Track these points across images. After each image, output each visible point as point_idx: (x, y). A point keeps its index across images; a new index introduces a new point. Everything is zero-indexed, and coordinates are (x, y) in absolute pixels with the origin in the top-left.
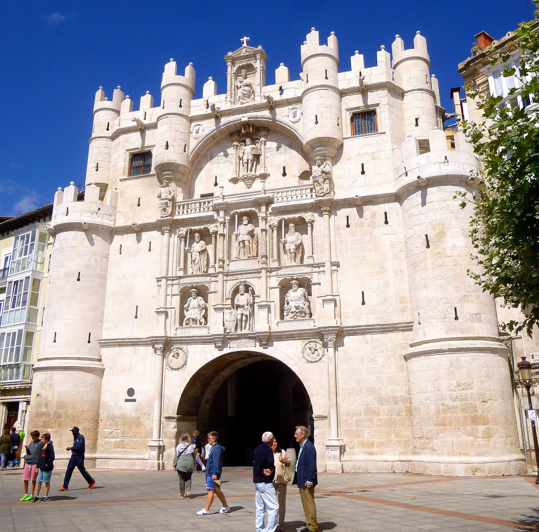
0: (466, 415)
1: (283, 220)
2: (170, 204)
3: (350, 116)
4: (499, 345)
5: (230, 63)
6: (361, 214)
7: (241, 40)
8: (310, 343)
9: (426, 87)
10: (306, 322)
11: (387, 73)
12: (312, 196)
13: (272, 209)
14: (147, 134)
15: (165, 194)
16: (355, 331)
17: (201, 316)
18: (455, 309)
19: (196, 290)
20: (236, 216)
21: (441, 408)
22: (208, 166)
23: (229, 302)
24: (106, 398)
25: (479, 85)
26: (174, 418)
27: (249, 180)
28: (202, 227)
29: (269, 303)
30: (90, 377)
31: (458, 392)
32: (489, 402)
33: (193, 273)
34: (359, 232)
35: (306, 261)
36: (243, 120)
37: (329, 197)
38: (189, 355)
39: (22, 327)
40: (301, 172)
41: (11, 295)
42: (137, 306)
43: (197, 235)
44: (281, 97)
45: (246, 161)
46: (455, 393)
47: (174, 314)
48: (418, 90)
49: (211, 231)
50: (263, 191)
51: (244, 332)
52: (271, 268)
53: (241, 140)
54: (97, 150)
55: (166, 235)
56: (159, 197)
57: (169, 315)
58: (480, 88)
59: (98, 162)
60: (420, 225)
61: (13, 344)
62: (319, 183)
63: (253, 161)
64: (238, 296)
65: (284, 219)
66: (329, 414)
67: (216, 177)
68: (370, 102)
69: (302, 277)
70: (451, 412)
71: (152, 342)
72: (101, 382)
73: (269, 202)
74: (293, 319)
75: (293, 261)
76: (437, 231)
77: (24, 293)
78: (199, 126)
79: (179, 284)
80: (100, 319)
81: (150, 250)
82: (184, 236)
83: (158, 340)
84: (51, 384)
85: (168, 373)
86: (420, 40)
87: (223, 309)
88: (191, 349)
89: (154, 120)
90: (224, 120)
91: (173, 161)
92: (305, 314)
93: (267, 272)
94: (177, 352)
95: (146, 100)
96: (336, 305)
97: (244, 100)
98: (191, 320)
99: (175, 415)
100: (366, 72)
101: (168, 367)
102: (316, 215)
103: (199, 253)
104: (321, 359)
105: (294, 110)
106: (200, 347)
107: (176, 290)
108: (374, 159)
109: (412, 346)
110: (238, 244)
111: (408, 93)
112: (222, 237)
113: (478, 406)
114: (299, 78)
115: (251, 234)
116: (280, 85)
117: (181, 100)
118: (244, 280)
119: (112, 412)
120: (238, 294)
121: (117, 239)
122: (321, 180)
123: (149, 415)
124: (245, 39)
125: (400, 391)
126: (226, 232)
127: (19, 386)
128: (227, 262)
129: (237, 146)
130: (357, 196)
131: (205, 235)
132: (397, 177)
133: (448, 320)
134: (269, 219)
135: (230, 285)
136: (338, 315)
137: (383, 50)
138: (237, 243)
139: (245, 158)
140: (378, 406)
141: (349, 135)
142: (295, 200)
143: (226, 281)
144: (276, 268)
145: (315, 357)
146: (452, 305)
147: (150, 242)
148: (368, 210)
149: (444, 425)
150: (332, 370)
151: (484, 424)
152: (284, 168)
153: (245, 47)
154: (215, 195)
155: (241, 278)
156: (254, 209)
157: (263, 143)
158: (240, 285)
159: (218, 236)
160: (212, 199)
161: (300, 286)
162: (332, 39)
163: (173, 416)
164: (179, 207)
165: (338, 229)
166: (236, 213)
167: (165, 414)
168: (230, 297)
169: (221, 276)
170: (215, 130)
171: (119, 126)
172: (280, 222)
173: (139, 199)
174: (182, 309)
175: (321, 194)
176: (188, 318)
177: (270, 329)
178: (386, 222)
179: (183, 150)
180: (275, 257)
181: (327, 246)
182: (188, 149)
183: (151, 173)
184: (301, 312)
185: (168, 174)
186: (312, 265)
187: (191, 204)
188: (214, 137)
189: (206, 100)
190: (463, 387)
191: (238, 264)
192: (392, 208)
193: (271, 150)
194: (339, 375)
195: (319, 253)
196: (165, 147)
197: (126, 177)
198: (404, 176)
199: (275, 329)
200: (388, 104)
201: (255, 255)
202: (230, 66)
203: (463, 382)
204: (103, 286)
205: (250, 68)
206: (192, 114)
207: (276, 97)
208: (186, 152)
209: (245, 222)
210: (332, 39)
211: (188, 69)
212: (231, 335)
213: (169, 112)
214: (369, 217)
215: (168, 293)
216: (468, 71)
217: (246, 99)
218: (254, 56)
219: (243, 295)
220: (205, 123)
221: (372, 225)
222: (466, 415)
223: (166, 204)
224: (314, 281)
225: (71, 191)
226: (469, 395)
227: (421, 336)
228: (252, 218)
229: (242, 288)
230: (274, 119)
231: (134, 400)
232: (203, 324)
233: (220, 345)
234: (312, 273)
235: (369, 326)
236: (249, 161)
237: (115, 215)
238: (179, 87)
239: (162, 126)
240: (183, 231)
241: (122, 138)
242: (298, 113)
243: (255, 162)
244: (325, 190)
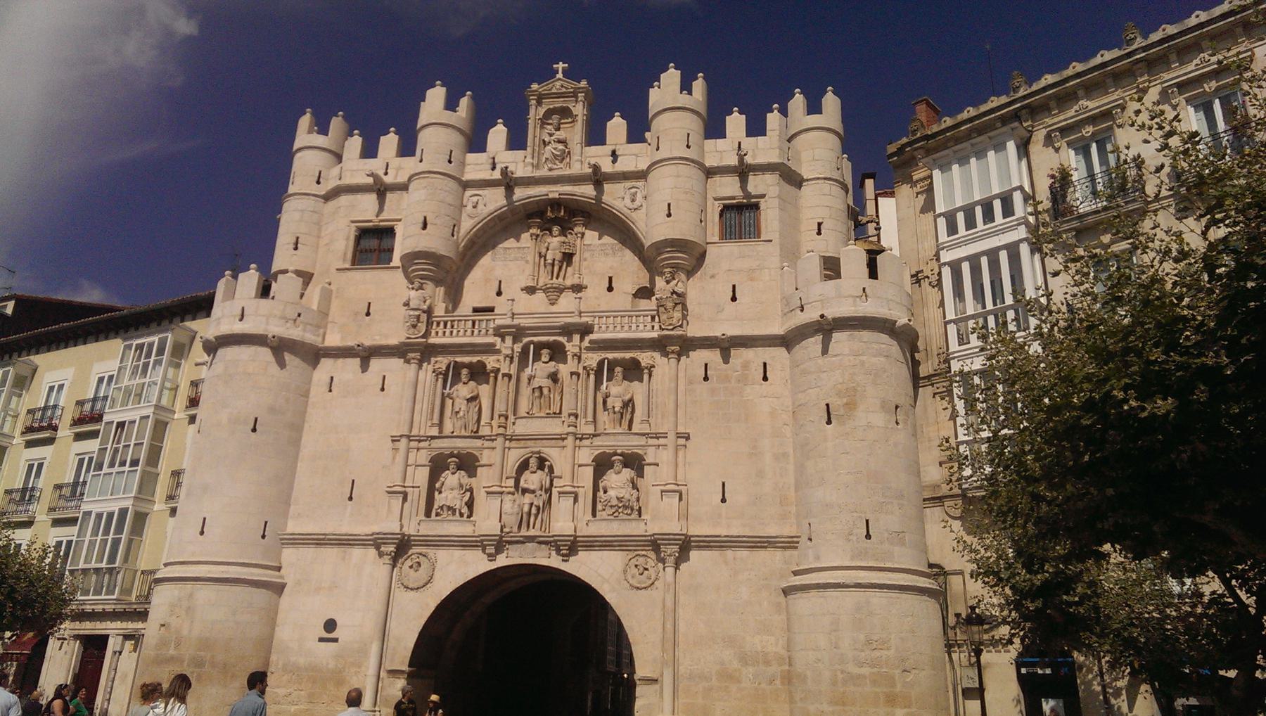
0: (877, 690)
2: (424, 317)
3: (720, 208)
4: (930, 583)
5: (535, 102)
6: (726, 359)
7: (555, 66)
8: (637, 558)
9: (836, 175)
10: (634, 524)
11: (780, 149)
13: (591, 342)
14: (387, 200)
15: (418, 302)
16: (708, 543)
17: (463, 504)
18: (867, 521)
19: (457, 460)
20: (532, 346)
21: (840, 676)
22: (486, 261)
23: (511, 482)
24: (284, 633)
25: (917, 181)
26: (402, 672)
27: (555, 293)
29: (576, 489)
30: (261, 596)
31: (868, 652)
32: (914, 671)
33: (453, 432)
35: (636, 428)
36: (551, 196)
37: (681, 332)
38: (438, 566)
39: (128, 504)
40: (638, 287)
41: (109, 446)
42: (353, 481)
43: (465, 372)
44: (614, 168)
45: (550, 261)
46: (863, 654)
47: (418, 497)
48: (825, 179)
49: (489, 367)
50: (577, 313)
51: (532, 532)
52: (583, 435)
53: (544, 228)
54: (297, 216)
55: (414, 367)
56: (407, 304)
57: (409, 498)
58: (918, 186)
59: (298, 235)
60: (818, 389)
61: (106, 532)
62: (665, 309)
63: (561, 262)
64: (526, 475)
65: (607, 358)
66: (662, 675)
67: (500, 282)
68: (750, 188)
70: (854, 685)
71: (377, 542)
72: (277, 605)
73: (586, 330)
74: (612, 517)
75: (618, 425)
76: (845, 400)
77: (135, 444)
78: (479, 197)
79: (430, 448)
80: (285, 500)
81: (383, 389)
84: (189, 608)
85: (400, 596)
86: (831, 102)
87: (502, 493)
88: (442, 555)
89: (402, 179)
90: (520, 193)
91: (433, 250)
92: (632, 510)
94: (417, 560)
95: (389, 142)
96: (680, 499)
97: (555, 164)
98: (445, 508)
99: (405, 668)
100: (749, 142)
101: (400, 585)
102: (657, 355)
104: (653, 583)
105: (633, 190)
106: (457, 553)
107: (424, 457)
108: (752, 279)
109: (796, 573)
111: (810, 183)
112: (506, 379)
113: (897, 678)
114: (643, 140)
115: (554, 377)
116: (613, 147)
117: (451, 152)
118: (538, 449)
119: (293, 659)
120: (526, 472)
121: (326, 365)
122: (670, 305)
123: (360, 667)
124: (561, 66)
125: (773, 644)
126: (513, 371)
127: (113, 607)
128: (511, 419)
129: (538, 236)
130: (724, 335)
131: (479, 373)
132: (786, 311)
133: (854, 538)
134: (584, 356)
135: (515, 456)
136: (684, 516)
137: (776, 111)
138: (530, 389)
139: (549, 257)
140: (740, 667)
141: (716, 239)
142: (626, 331)
143: (509, 449)
144: (590, 435)
145: (643, 580)
146: (863, 516)
147: (384, 377)
148: (738, 356)
149: (844, 704)
150: (669, 604)
151: (905, 707)
152: (610, 279)
153: (559, 79)
154: (496, 311)
155: (535, 447)
156: (560, 339)
157: (579, 235)
158: (531, 457)
159: (500, 376)
160: (494, 317)
161: (625, 465)
162: (699, 86)
163: (399, 668)
164: (438, 324)
165: (691, 383)
166: (532, 342)
167: (388, 665)
168: (514, 475)
169: (500, 439)
170: (504, 207)
171: (340, 179)
172: (601, 363)
173: (370, 303)
174: (431, 490)
177: (575, 531)
178: (765, 378)
179: (450, 234)
180: (590, 418)
181: (671, 406)
182: (458, 233)
183: (392, 264)
184: (625, 507)
185: (424, 270)
187: (459, 321)
188: (501, 218)
189: (491, 156)
190: (875, 646)
192: (776, 356)
193: (592, 248)
194: (680, 611)
195: (660, 416)
196: (421, 225)
197: (348, 266)
198: (798, 311)
199: (584, 531)
200: (779, 197)
201: (558, 412)
202: (534, 107)
203: (875, 638)
204: (296, 443)
205: (565, 113)
206: (467, 177)
207: (607, 166)
208: (455, 237)
209: (545, 358)
210: (699, 86)
211: (464, 102)
212: (512, 537)
213: (431, 170)
214: (739, 368)
215: (409, 463)
216: (902, 157)
217: (557, 162)
218: (575, 95)
219: (535, 472)
220: (487, 192)
221: (744, 380)
222: (877, 690)
223: (418, 317)
224: (649, 459)
225: (250, 279)
226: (884, 657)
227: (811, 559)
228: (557, 353)
229: (533, 462)
230: (598, 199)
231: (336, 640)
232: (465, 516)
235: (732, 537)
236: (556, 262)
237: (326, 327)
238: (449, 131)
239: (418, 191)
240: (442, 362)
241: (344, 200)
242: (639, 197)
243: (565, 263)
244: (675, 321)
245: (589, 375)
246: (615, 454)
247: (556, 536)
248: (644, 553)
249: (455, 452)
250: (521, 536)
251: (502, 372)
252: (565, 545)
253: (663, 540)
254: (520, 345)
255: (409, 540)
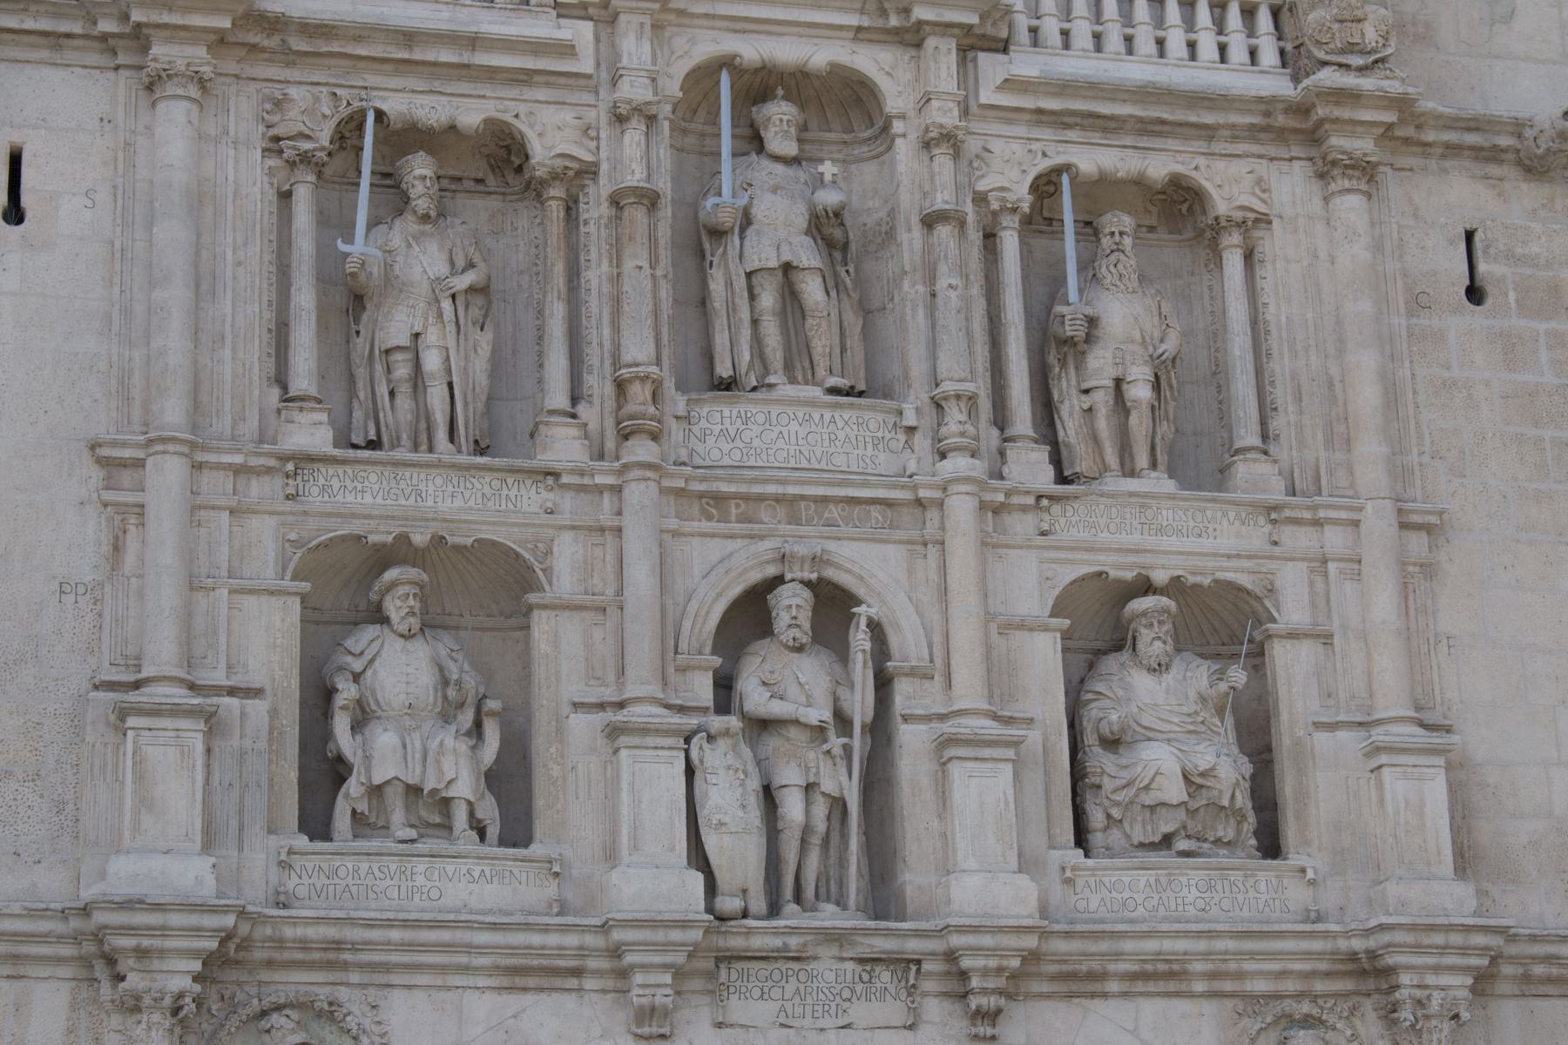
1: (1065, 179)
12: (1253, 53)
13: (1009, 84)
19: (425, 576)
20: (725, 79)
23: (702, 689)
28: (471, 115)
34: (1542, 341)
65: (1067, 168)
69: (1206, 581)
82: (322, 155)
83: (163, 931)
93: (983, 506)
98: (395, 798)
103: (447, 305)
110: (740, 283)
112: (637, 215)
120: (762, 646)
158: (778, 580)
159: (595, 209)
166: (727, 63)
172: (1045, 186)
175: (1342, 52)
176: (377, 780)
186: (1275, 508)
191: (756, 429)
212: (749, 932)
219: (800, 649)
224: (1293, 609)
229: (792, 605)
232: (493, 831)
233: (659, 1000)
234: (1271, 558)
245: (990, 237)
246: (1146, 587)
247: (961, 930)
248: (1306, 1007)
249: (419, 539)
250: (793, 931)
251: (603, 187)
252: (999, 970)
253: (1417, 949)
254: (682, 68)
255: (246, 944)
